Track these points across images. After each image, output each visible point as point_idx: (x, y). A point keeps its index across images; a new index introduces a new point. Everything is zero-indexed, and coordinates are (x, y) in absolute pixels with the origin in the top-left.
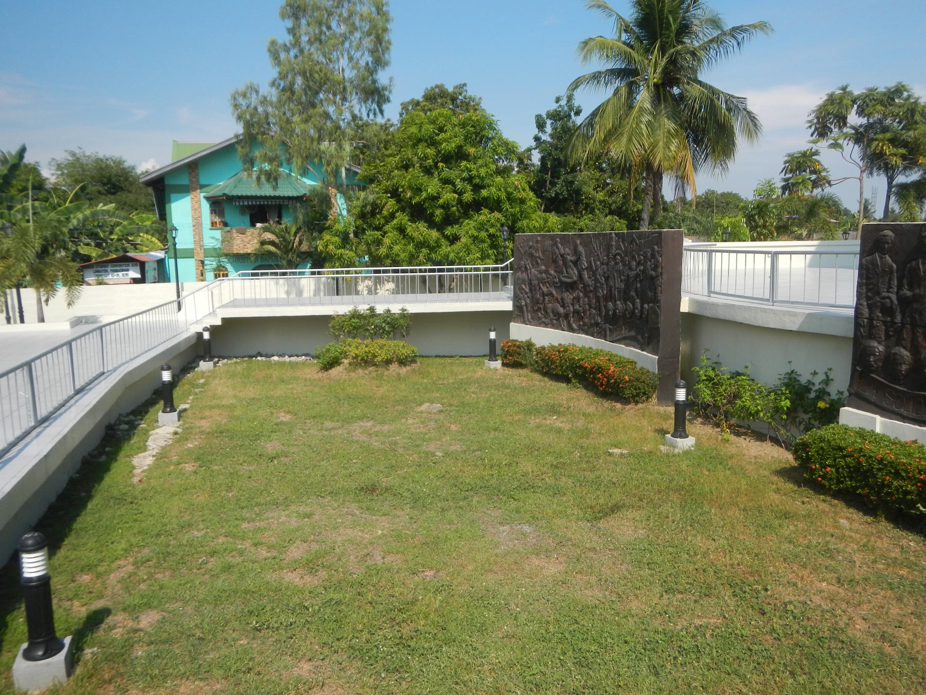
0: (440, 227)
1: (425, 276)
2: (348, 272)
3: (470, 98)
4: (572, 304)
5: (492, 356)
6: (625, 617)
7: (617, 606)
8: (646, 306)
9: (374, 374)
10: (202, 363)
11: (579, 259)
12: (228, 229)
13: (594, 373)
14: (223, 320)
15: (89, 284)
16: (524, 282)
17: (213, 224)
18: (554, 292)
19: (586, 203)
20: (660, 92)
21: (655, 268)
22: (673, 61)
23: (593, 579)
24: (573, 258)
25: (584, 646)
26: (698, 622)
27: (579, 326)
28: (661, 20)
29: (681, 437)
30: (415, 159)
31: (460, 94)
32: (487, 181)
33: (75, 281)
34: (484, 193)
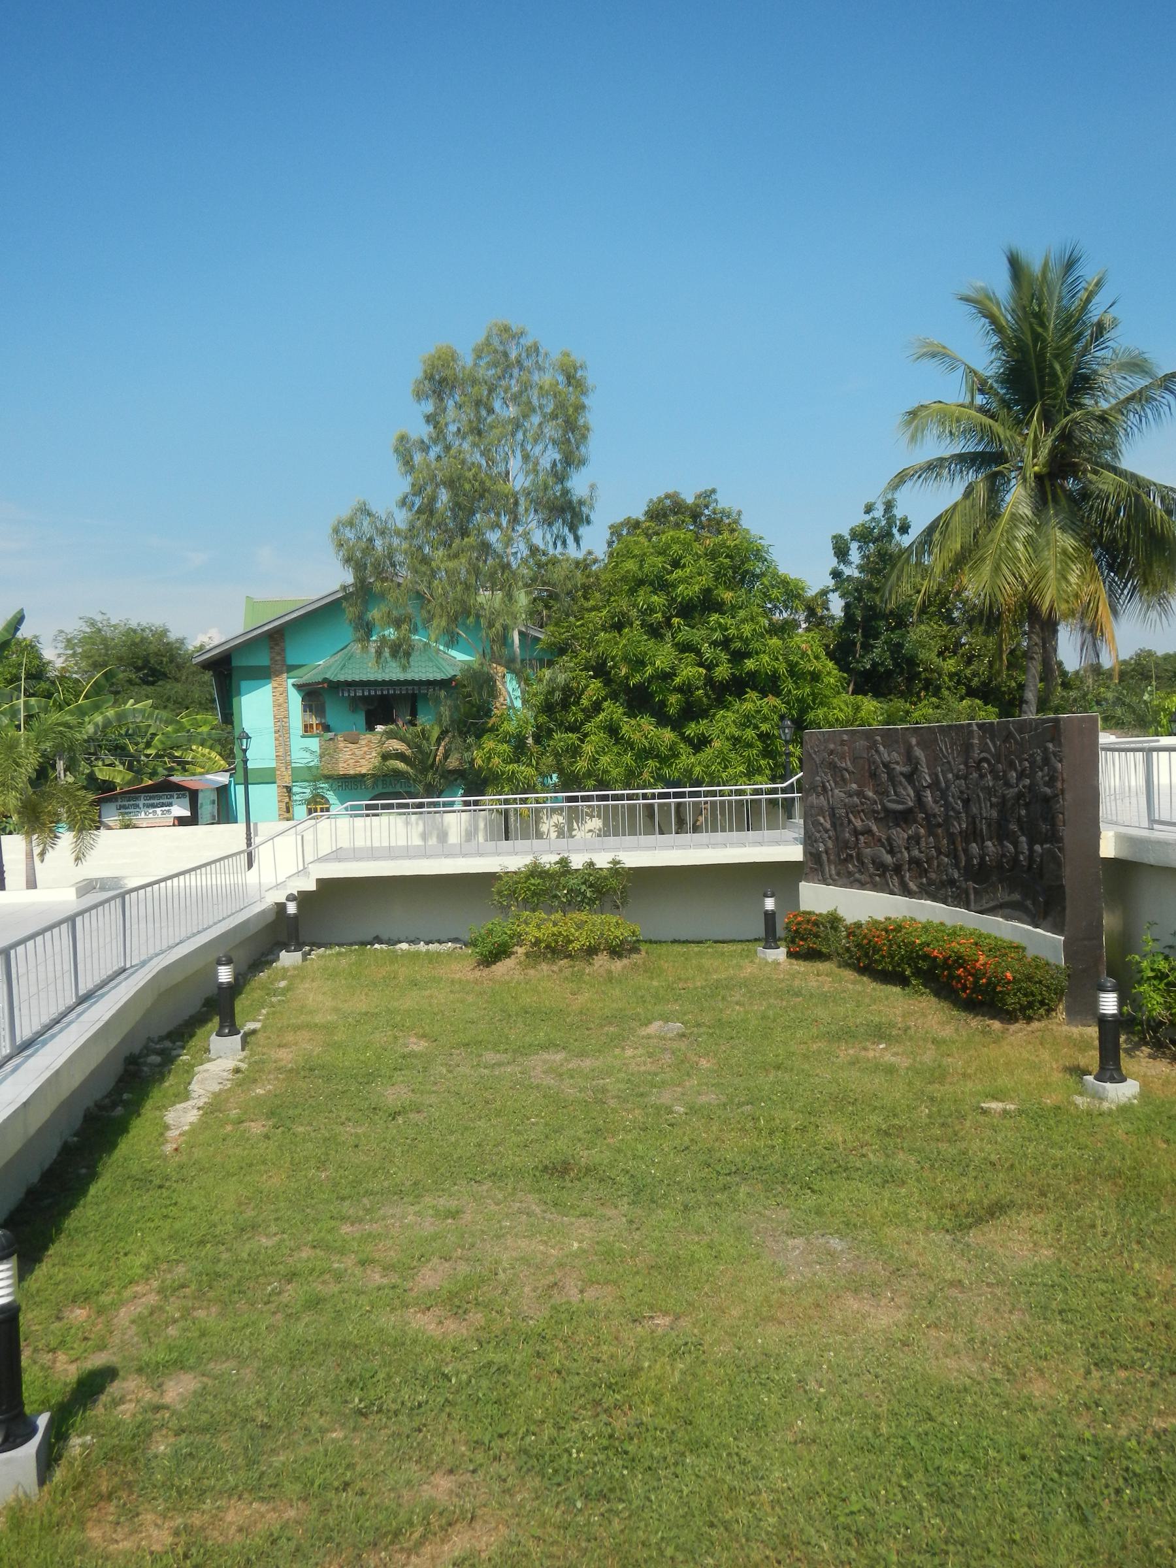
0: (677, 724)
1: (652, 805)
2: (524, 801)
3: (723, 512)
4: (907, 849)
5: (770, 940)
6: (1021, 1410)
7: (1007, 1390)
8: (1038, 848)
9: (567, 972)
10: (283, 954)
11: (915, 770)
12: (331, 735)
13: (949, 968)
14: (320, 881)
15: (109, 828)
16: (821, 811)
17: (307, 728)
18: (875, 828)
19: (926, 679)
20: (1046, 488)
21: (1052, 781)
22: (1066, 437)
23: (959, 1339)
24: (906, 769)
25: (946, 1463)
26: (1158, 1423)
27: (920, 886)
28: (1041, 370)
29: (1113, 1080)
30: (634, 613)
31: (707, 507)
32: (755, 645)
33: (87, 824)
34: (750, 664)
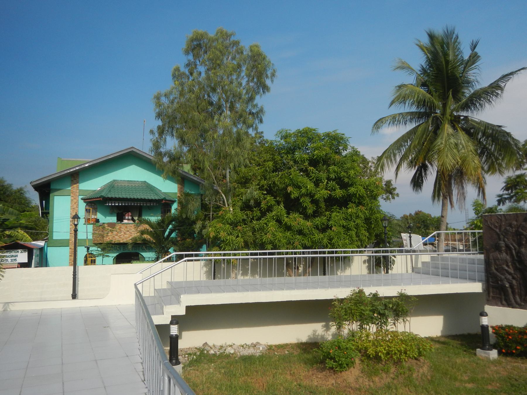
14: (188, 308)
34: (352, 190)
